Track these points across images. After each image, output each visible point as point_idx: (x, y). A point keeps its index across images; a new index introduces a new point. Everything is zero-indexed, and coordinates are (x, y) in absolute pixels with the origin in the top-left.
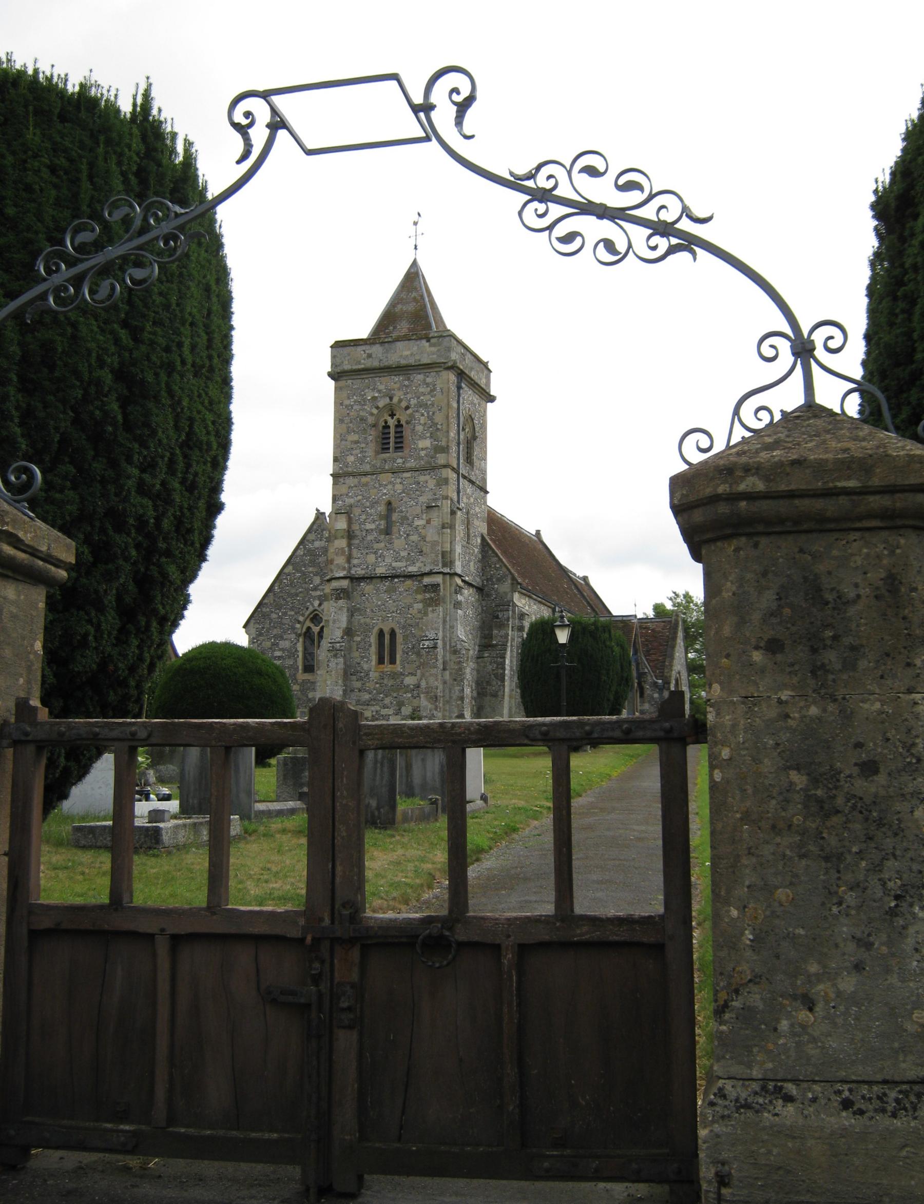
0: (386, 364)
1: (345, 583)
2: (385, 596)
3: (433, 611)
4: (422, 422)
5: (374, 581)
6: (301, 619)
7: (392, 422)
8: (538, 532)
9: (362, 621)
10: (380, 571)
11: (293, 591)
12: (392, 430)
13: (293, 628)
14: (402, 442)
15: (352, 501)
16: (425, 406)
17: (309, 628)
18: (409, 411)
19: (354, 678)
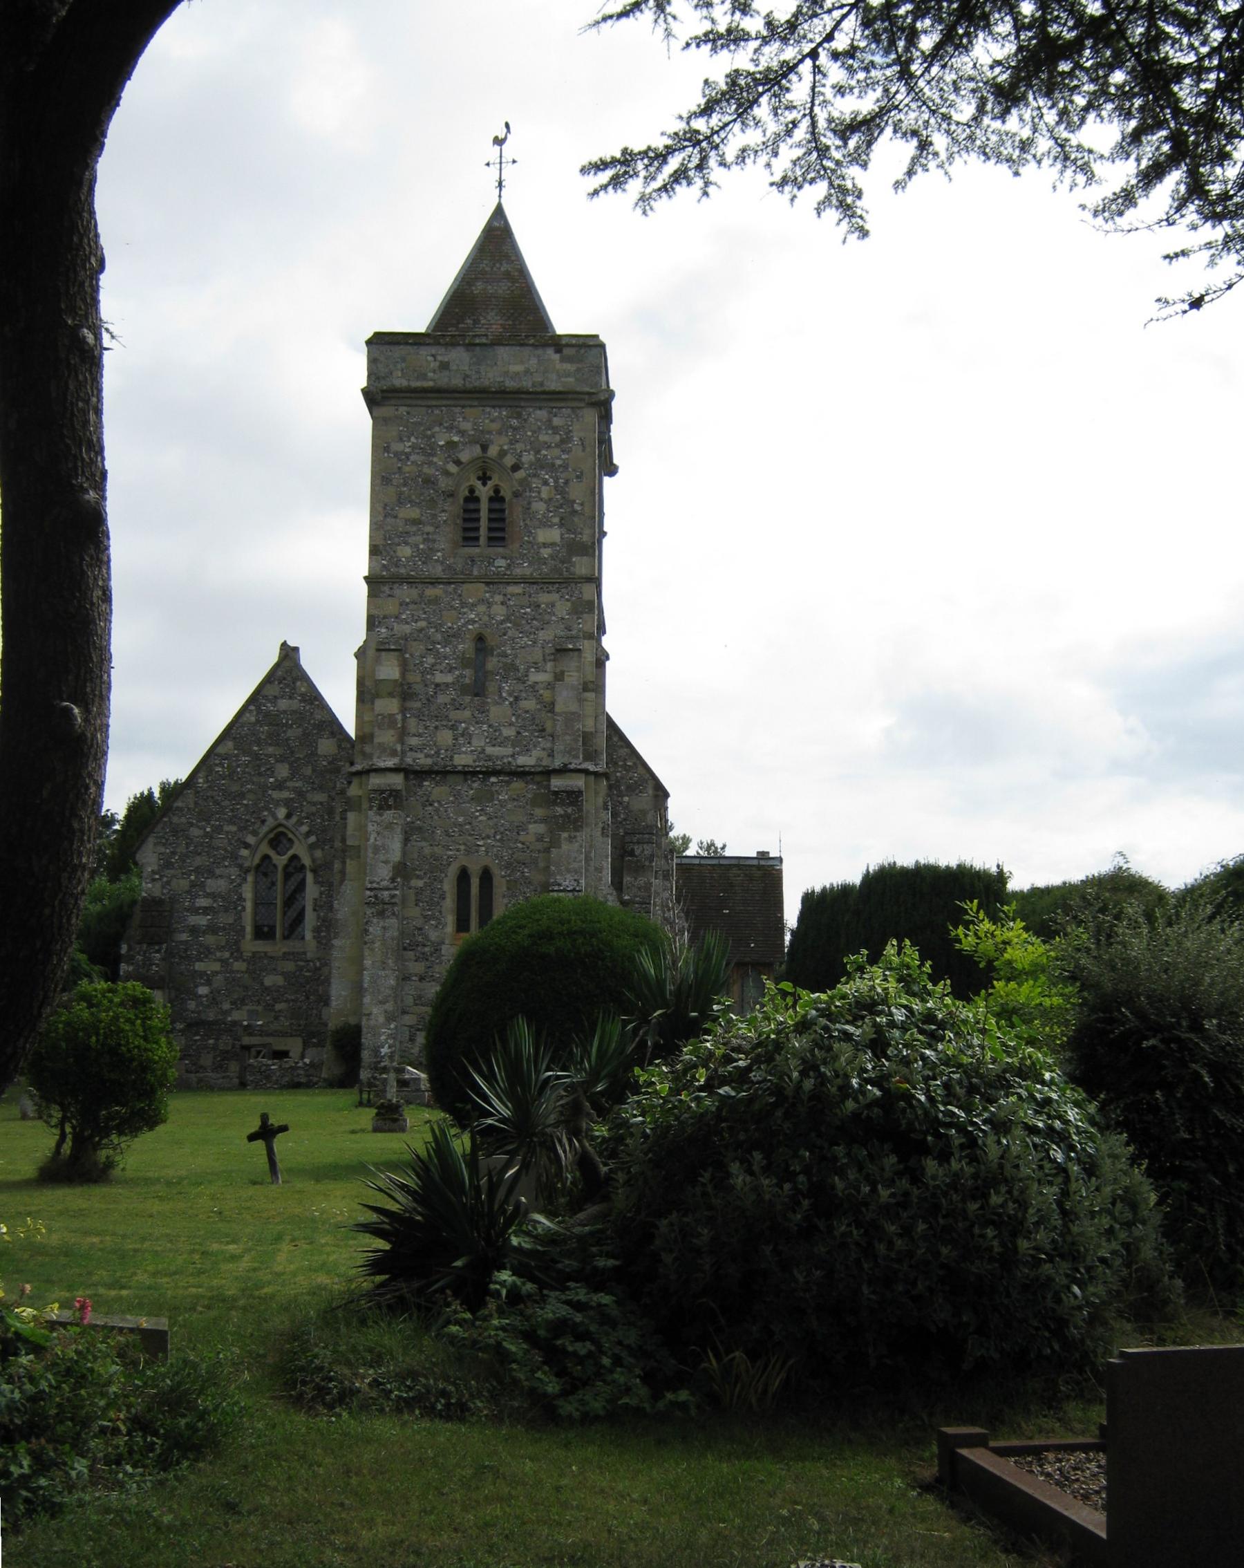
0: (477, 384)
1: (397, 780)
2: (473, 808)
3: (571, 839)
4: (544, 495)
5: (451, 778)
6: (251, 840)
7: (484, 492)
9: (427, 851)
10: (462, 760)
11: (235, 788)
12: (484, 506)
13: (234, 857)
14: (503, 530)
15: (407, 629)
16: (552, 467)
17: (266, 858)
18: (520, 474)
19: (411, 954)
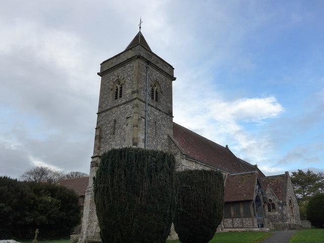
8: (227, 146)
